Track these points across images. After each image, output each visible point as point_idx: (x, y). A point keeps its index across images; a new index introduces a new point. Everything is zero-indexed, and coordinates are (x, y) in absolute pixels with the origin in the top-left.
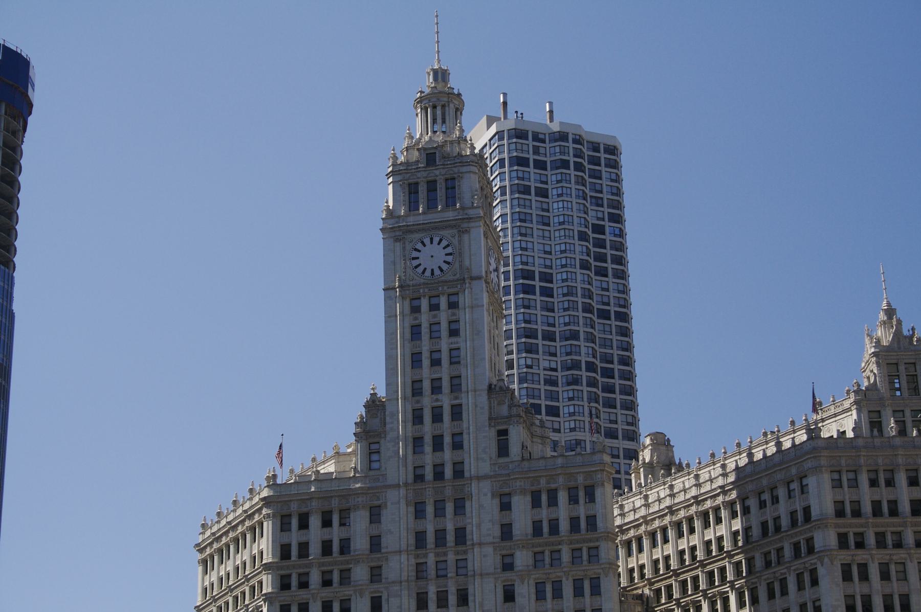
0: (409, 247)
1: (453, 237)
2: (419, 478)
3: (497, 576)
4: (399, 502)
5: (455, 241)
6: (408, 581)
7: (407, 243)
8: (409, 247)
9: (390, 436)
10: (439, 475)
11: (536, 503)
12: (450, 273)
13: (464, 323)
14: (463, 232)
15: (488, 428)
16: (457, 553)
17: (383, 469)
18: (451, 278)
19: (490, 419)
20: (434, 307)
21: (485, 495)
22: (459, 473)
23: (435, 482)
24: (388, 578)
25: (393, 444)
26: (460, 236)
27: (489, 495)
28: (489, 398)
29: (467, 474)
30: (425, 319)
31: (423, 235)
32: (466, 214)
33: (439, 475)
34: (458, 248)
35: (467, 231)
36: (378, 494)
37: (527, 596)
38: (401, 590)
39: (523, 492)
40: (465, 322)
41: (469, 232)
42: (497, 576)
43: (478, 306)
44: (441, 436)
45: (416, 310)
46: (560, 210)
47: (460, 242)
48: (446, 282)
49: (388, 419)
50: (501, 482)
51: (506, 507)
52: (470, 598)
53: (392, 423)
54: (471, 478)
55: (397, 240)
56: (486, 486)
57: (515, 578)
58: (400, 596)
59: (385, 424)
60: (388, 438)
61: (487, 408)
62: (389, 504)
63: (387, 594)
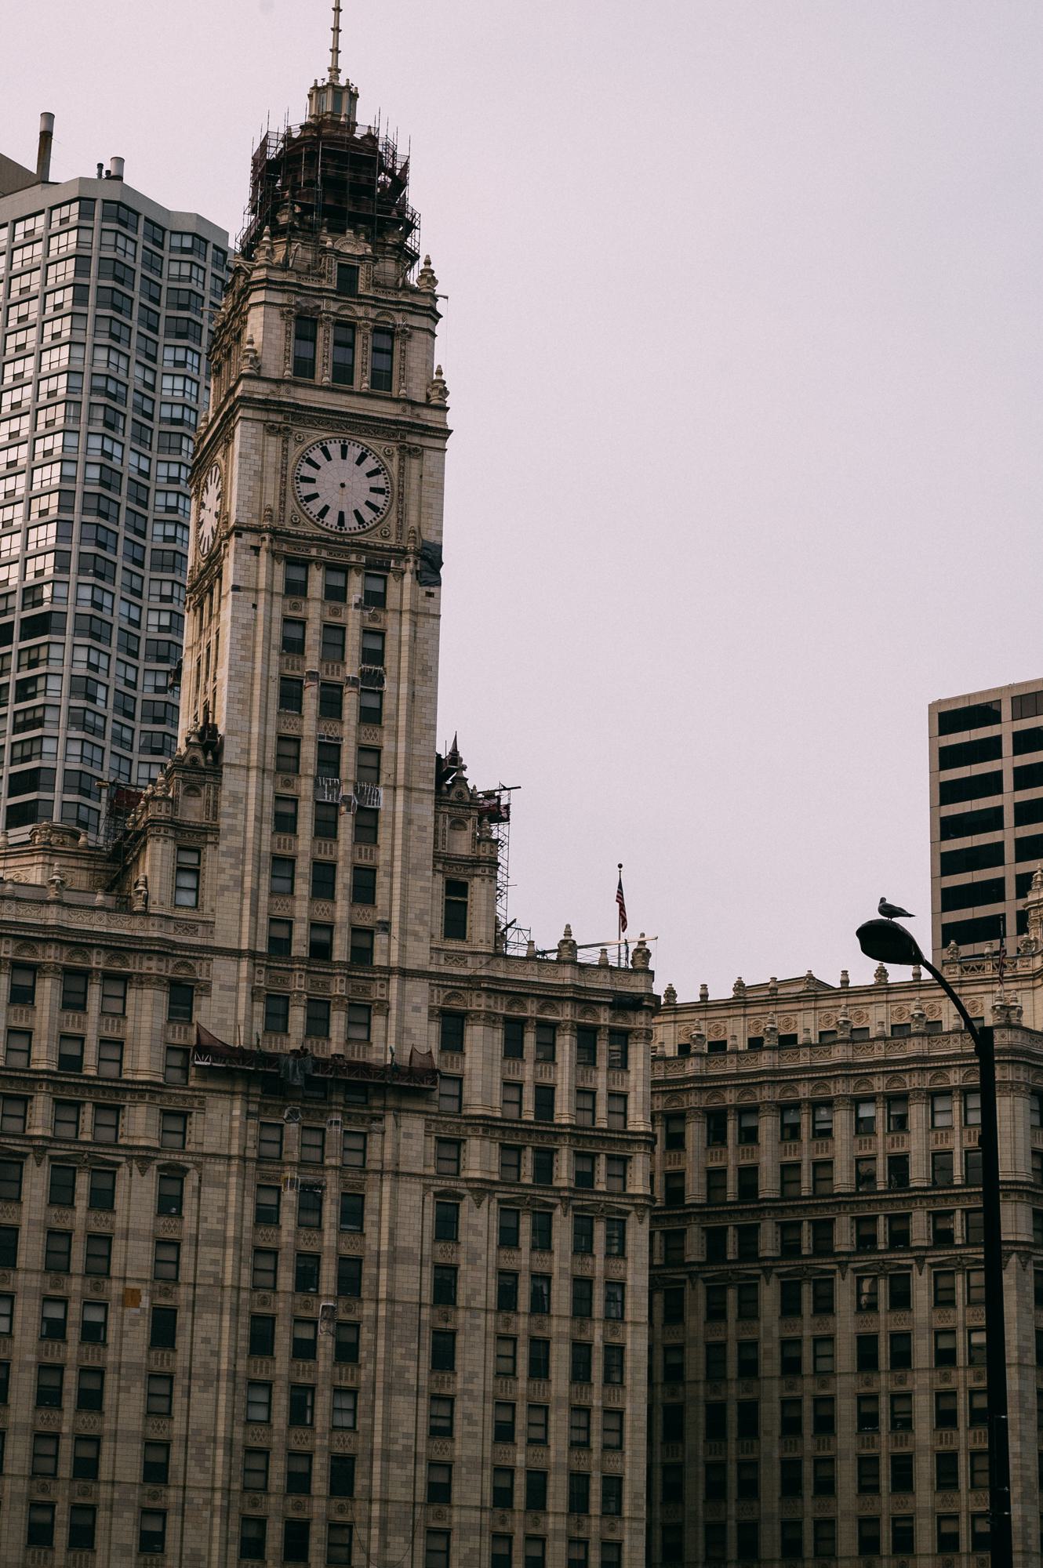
0: (295, 451)
1: (389, 456)
2: (280, 946)
3: (428, 1181)
4: (236, 989)
5: (393, 467)
6: (244, 1159)
7: (292, 444)
8: (295, 451)
9: (226, 843)
10: (321, 951)
11: (513, 1050)
12: (377, 531)
13: (396, 643)
14: (409, 452)
15: (430, 873)
16: (347, 1117)
17: (207, 910)
18: (379, 541)
19: (437, 857)
20: (336, 595)
21: (417, 1009)
22: (362, 954)
23: (314, 961)
24: (202, 1144)
25: (232, 861)
26: (402, 459)
27: (425, 1010)
28: (436, 813)
29: (379, 960)
30: (314, 612)
31: (325, 435)
32: (418, 416)
33: (321, 951)
34: (395, 483)
35: (416, 452)
36: (190, 961)
37: (485, 1234)
38: (229, 1174)
39: (490, 1019)
40: (400, 642)
41: (422, 454)
42: (428, 1181)
43: (427, 615)
44: (332, 867)
45: (296, 589)
46: (176, 393)
47: (402, 470)
48: (367, 546)
49: (225, 806)
50: (449, 991)
52: (369, 1218)
53: (234, 816)
54: (389, 970)
55: (271, 430)
56: (419, 993)
57: (465, 1192)
58: (226, 1186)
59: (216, 815)
60: (222, 847)
61: (431, 830)
62: (215, 987)
63: (196, 1178)
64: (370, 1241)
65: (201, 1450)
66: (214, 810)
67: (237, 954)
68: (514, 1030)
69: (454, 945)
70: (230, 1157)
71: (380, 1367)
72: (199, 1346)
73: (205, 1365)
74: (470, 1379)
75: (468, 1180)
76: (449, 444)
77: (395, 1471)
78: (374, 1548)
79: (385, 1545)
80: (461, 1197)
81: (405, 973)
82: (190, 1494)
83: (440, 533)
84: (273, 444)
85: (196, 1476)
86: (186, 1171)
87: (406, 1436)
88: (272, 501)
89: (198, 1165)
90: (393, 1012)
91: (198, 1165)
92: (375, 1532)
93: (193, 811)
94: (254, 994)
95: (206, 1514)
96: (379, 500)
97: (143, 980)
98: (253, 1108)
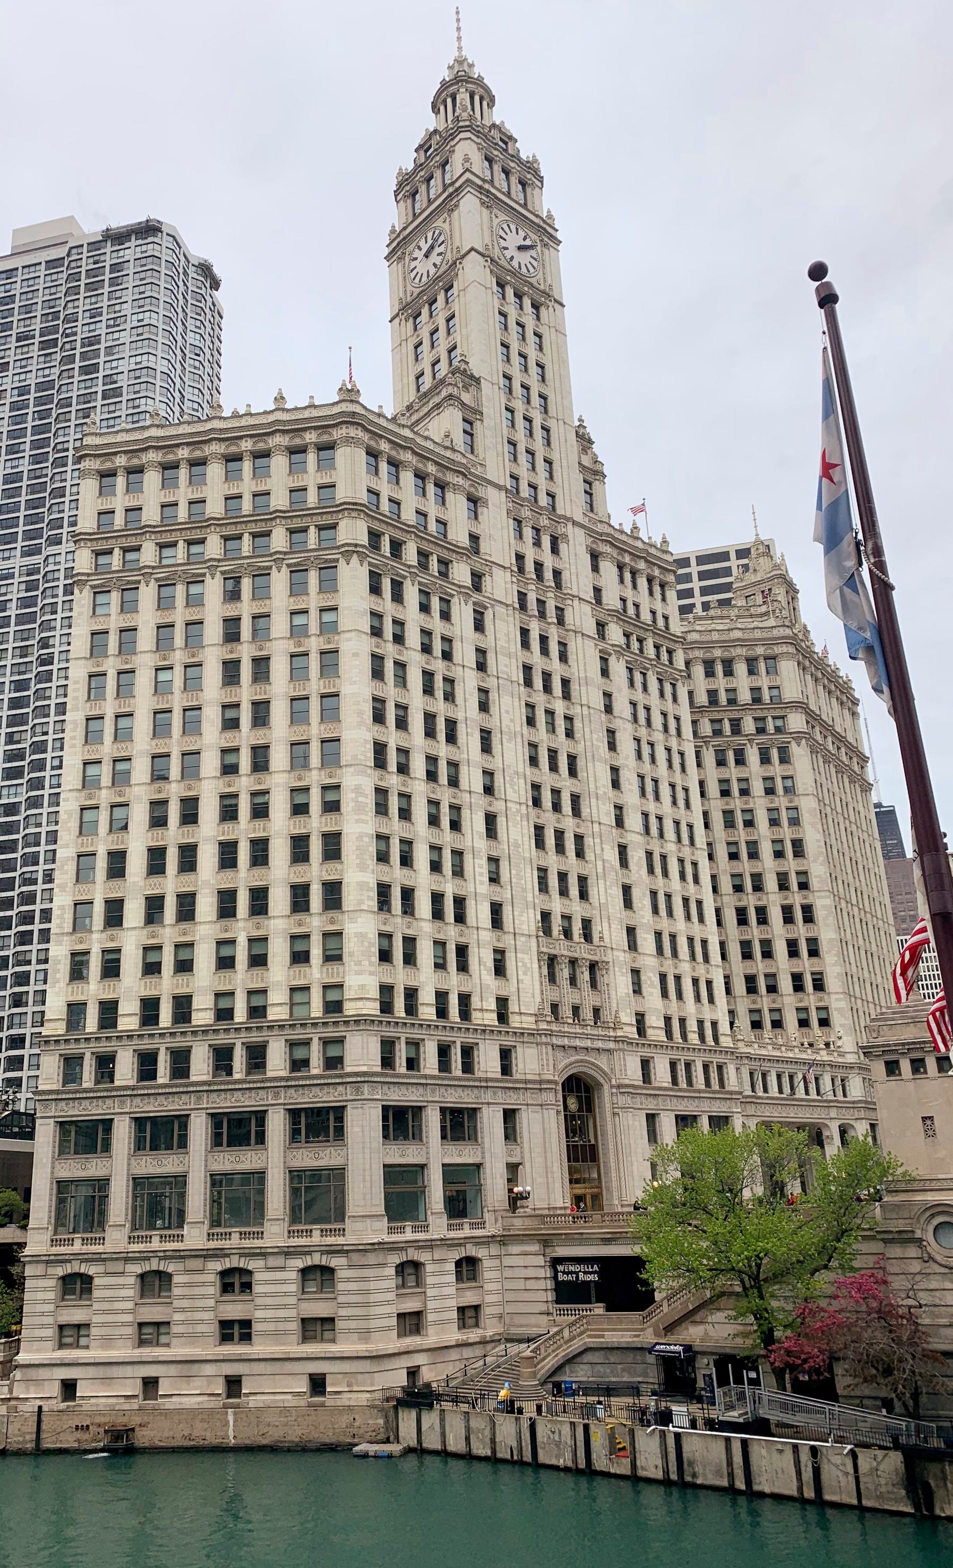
8: (496, 221)
51: (595, 568)
54: (568, 519)
60: (486, 421)
64: (574, 669)
65: (512, 779)
66: (478, 400)
67: (499, 487)
68: (621, 567)
69: (591, 515)
70: (507, 605)
71: (588, 743)
72: (503, 714)
73: (508, 726)
74: (627, 757)
75: (613, 645)
76: (559, 248)
77: (601, 806)
78: (598, 849)
79: (602, 850)
80: (610, 655)
81: (575, 523)
82: (509, 804)
83: (561, 293)
84: (485, 212)
85: (511, 795)
86: (486, 608)
87: (604, 786)
88: (487, 241)
89: (493, 606)
90: (571, 542)
91: (493, 606)
92: (597, 840)
93: (466, 397)
94: (509, 512)
95: (519, 818)
96: (535, 264)
97: (456, 488)
98: (514, 580)
